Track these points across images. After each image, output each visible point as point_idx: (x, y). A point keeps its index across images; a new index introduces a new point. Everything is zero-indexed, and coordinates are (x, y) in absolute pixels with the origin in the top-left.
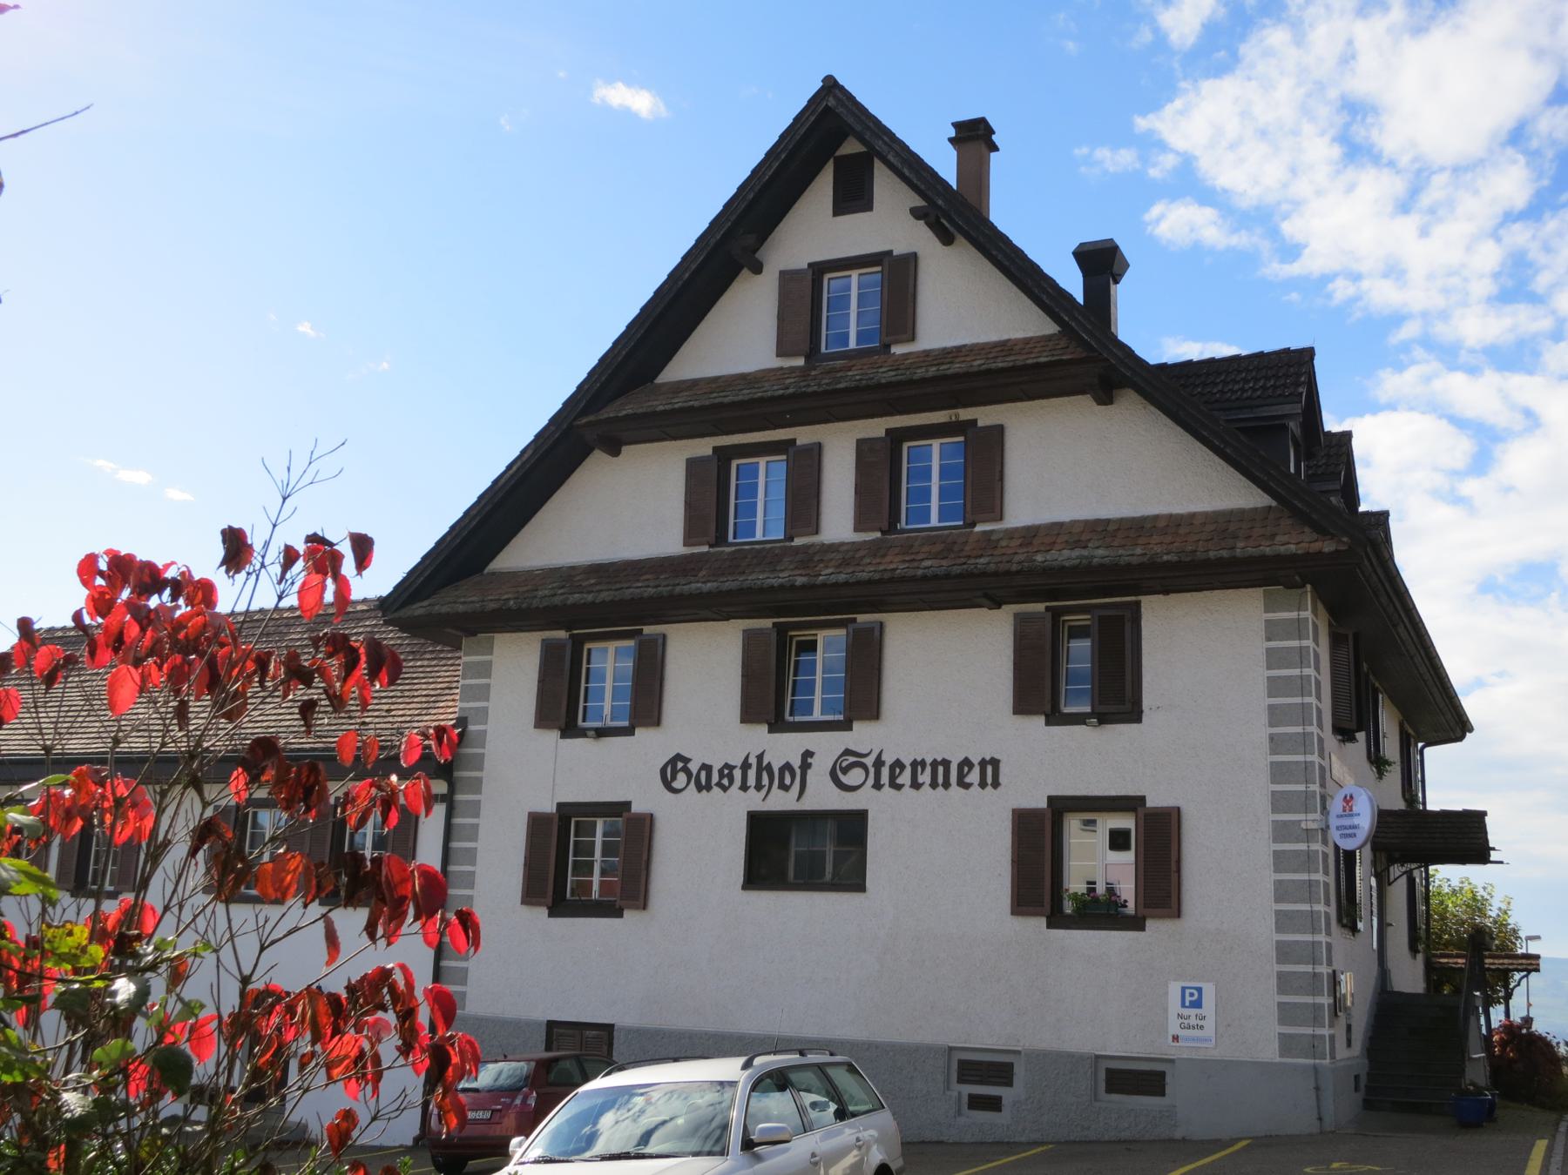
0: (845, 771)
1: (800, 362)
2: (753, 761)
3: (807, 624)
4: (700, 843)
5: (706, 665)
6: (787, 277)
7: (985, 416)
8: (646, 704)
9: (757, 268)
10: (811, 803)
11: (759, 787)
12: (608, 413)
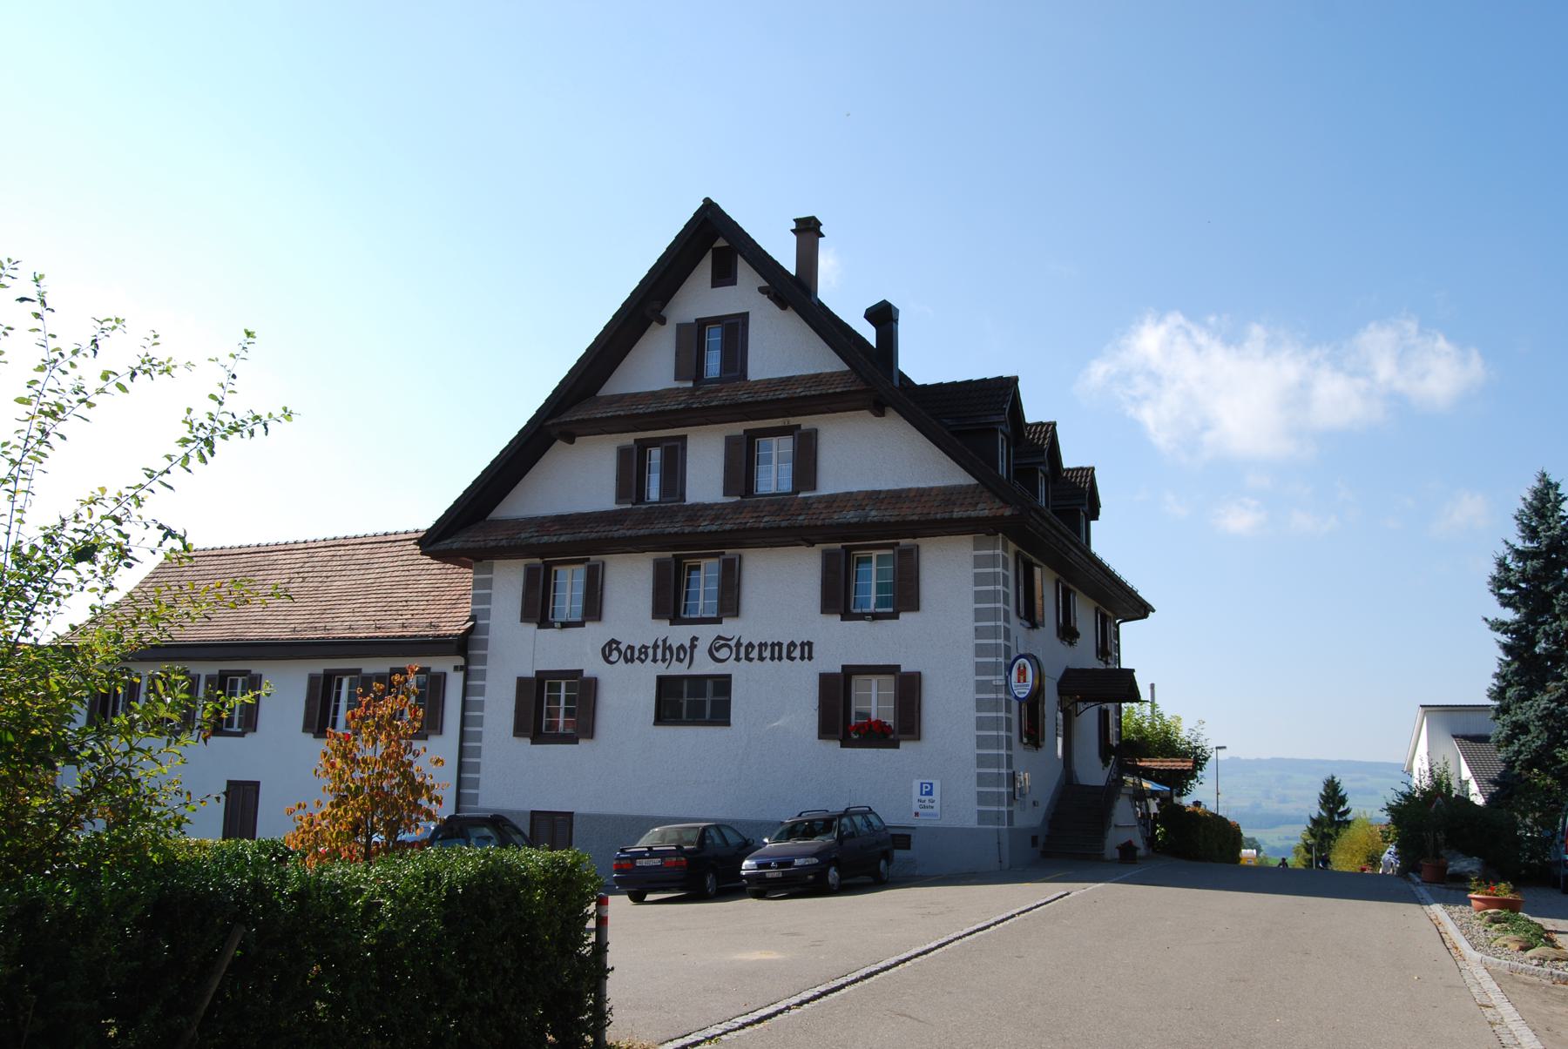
0: (717, 649)
1: (690, 384)
2: (660, 643)
3: (692, 553)
4: (627, 695)
5: (630, 580)
6: (681, 328)
7: (806, 422)
8: (593, 609)
9: (663, 321)
10: (696, 670)
11: (664, 660)
12: (566, 418)
